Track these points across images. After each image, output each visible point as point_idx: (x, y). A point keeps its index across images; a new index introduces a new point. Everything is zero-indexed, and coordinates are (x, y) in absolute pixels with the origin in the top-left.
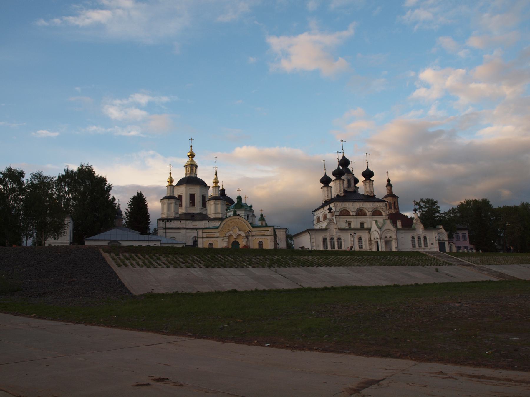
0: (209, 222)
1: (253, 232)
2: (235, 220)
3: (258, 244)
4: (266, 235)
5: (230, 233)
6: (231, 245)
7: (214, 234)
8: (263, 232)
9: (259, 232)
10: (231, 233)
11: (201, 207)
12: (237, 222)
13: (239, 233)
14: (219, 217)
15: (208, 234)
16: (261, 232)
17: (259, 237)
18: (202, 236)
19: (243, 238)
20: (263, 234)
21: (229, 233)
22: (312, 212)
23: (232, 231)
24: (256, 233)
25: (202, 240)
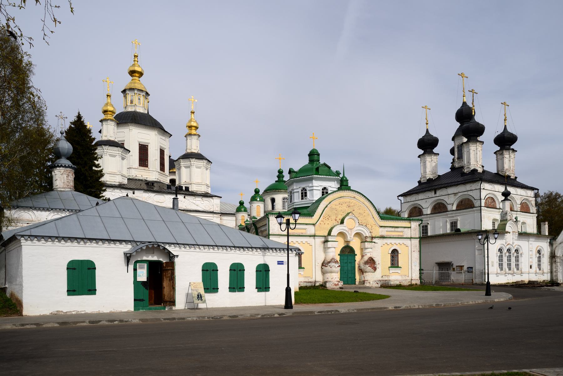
0: (186, 197)
2: (347, 200)
6: (339, 255)
7: (305, 229)
8: (399, 229)
9: (393, 229)
10: (344, 228)
11: (159, 171)
12: (352, 204)
14: (202, 191)
16: (396, 229)
20: (401, 234)
22: (398, 197)
24: (387, 231)
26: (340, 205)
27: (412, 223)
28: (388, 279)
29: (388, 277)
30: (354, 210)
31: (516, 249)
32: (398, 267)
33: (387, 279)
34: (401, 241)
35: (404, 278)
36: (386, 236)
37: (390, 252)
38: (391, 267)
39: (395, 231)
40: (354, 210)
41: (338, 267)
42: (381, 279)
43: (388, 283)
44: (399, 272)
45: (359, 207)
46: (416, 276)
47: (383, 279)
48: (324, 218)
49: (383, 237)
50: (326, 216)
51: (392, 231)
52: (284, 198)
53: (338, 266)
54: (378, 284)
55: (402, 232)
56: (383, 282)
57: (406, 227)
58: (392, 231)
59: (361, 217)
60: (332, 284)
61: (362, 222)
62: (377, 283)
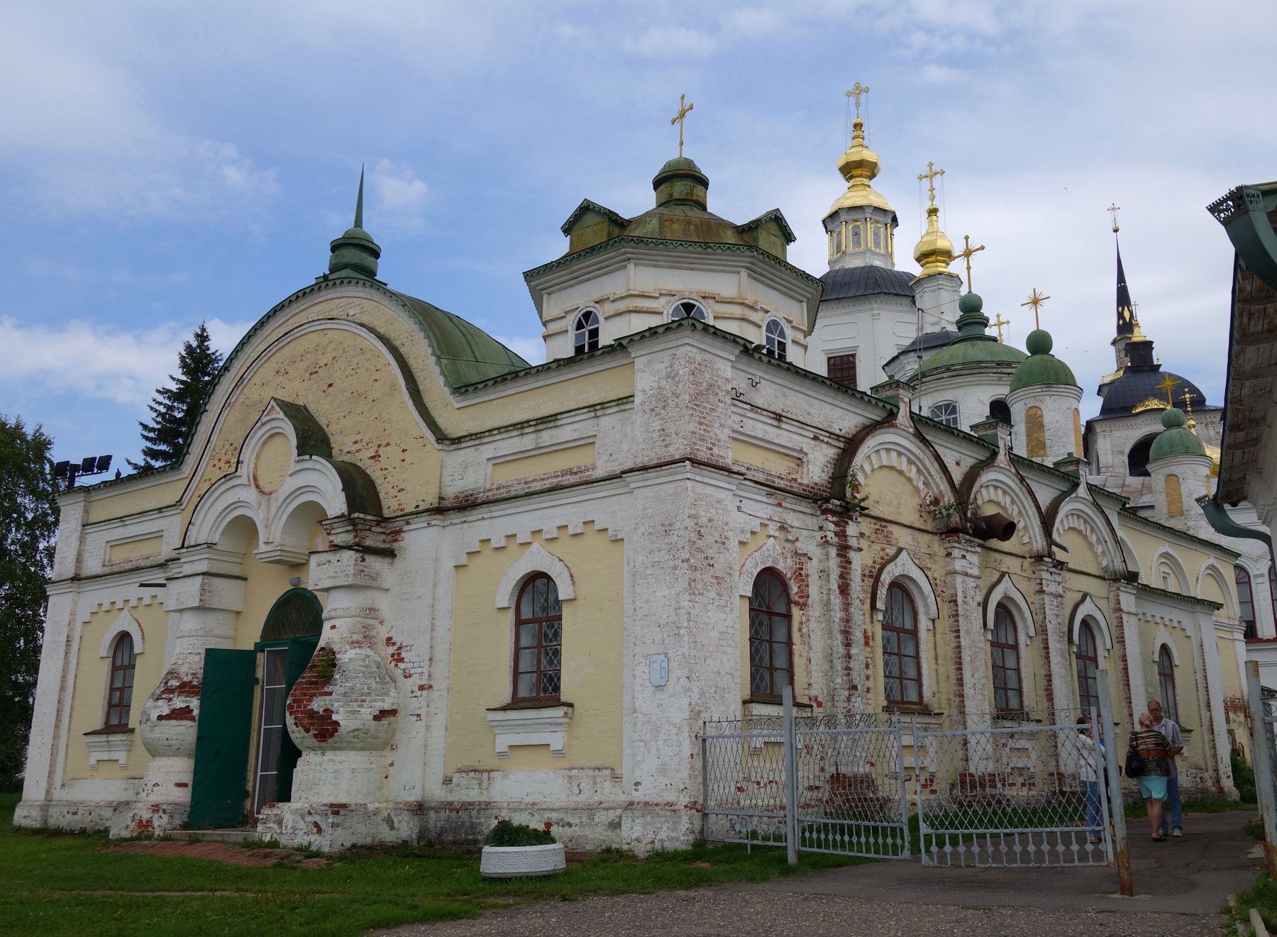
1: (466, 454)
3: (510, 617)
4: (600, 473)
5: (232, 497)
9: (527, 441)
12: (327, 358)
13: (301, 480)
15: (118, 532)
16: (548, 437)
17: (521, 520)
18: (79, 560)
19: (335, 548)
21: (221, 504)
23: (243, 470)
24: (497, 462)
25: (75, 603)
26: (281, 378)
27: (639, 363)
28: (484, 798)
29: (485, 784)
30: (330, 385)
31: (769, 324)
32: (557, 703)
33: (473, 795)
34: (569, 509)
35: (587, 797)
36: (482, 497)
37: (504, 596)
38: (516, 703)
39: (539, 452)
40: (330, 385)
41: (160, 718)
42: (438, 793)
43: (472, 826)
44: (557, 740)
45: (355, 361)
46: (663, 770)
47: (450, 798)
48: (216, 462)
49: (467, 504)
50: (224, 451)
51: (523, 456)
52: (954, 407)
53: (166, 711)
54: (320, 831)
55: (587, 443)
56: (443, 815)
57: (603, 405)
58: (523, 456)
59: (358, 410)
60: (129, 823)
61: (359, 437)
62: (316, 824)
